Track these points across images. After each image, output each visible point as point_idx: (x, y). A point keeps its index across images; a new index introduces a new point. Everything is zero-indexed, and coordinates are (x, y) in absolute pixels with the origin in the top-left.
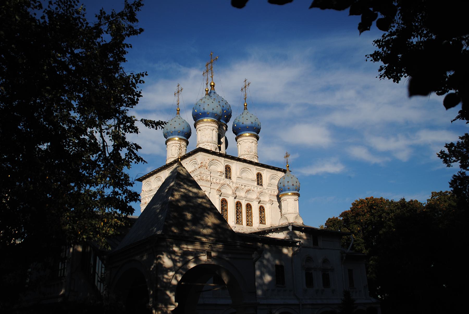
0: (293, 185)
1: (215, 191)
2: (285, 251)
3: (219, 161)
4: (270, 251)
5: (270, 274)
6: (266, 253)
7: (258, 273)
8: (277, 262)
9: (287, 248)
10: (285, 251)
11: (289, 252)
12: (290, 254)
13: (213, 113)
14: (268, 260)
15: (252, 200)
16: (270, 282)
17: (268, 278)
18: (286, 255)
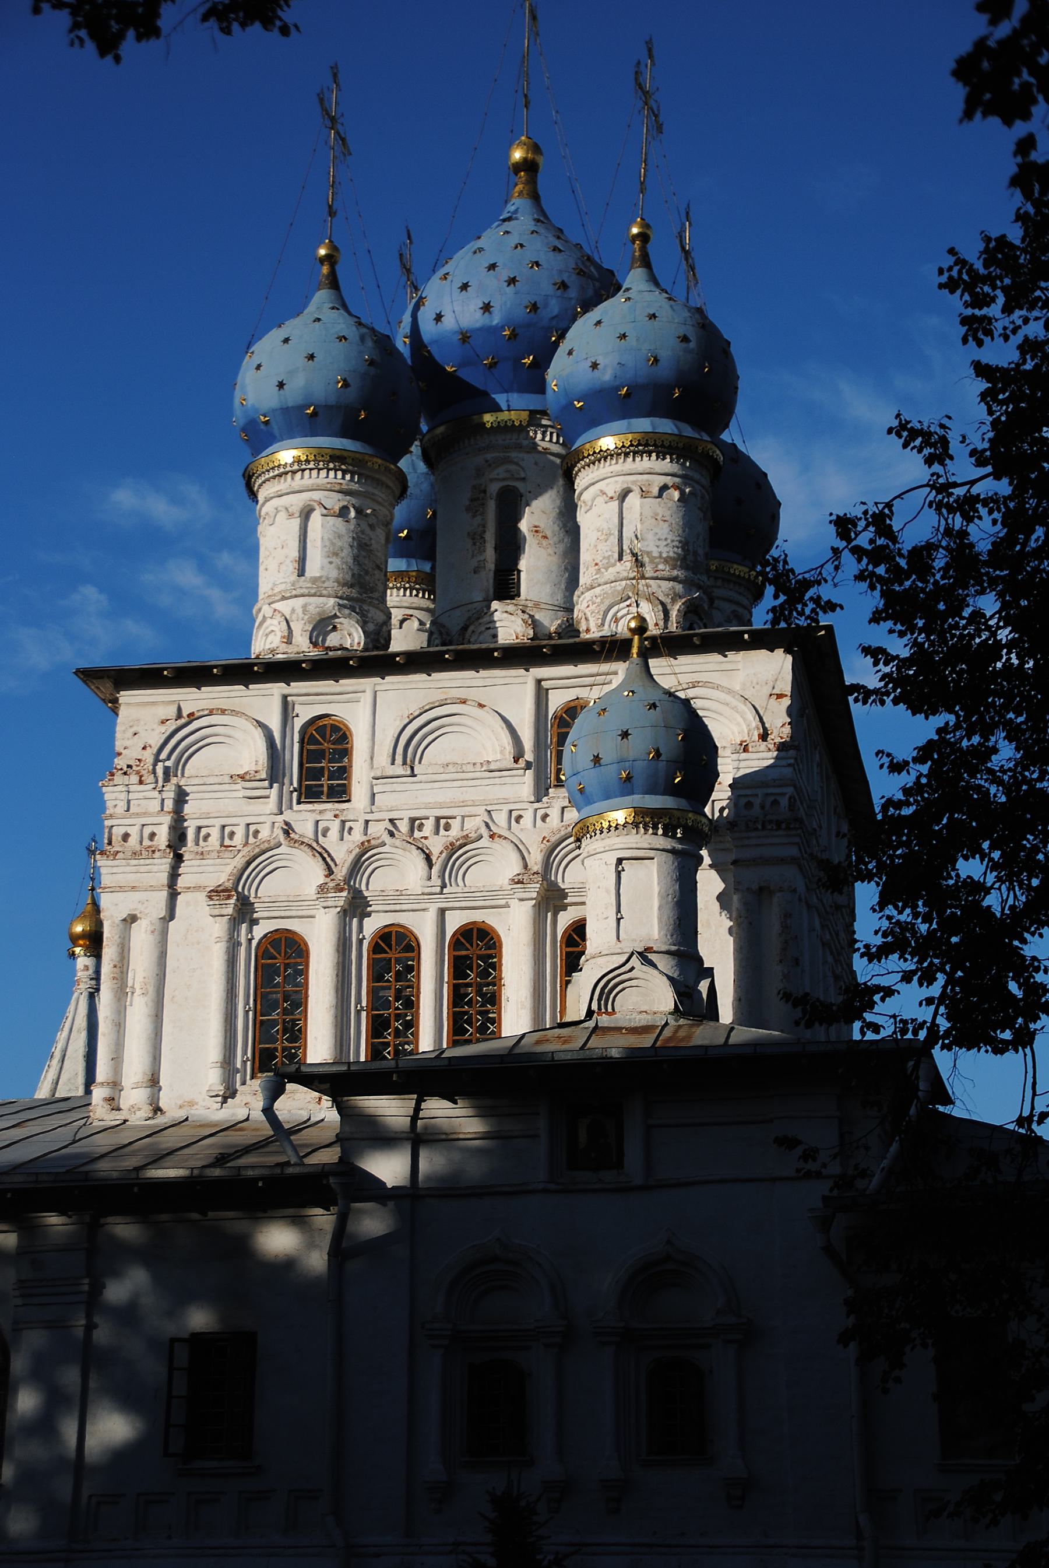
0: (597, 760)
1: (202, 896)
2: (278, 1240)
3: (234, 713)
4: (145, 1256)
5: (127, 1400)
6: (116, 1273)
7: (26, 1402)
8: (199, 1319)
9: (299, 1222)
10: (278, 1240)
11: (311, 1245)
12: (317, 1261)
13: (285, 410)
14: (128, 1315)
15: (495, 902)
16: (122, 1457)
17: (112, 1428)
18: (287, 1265)
